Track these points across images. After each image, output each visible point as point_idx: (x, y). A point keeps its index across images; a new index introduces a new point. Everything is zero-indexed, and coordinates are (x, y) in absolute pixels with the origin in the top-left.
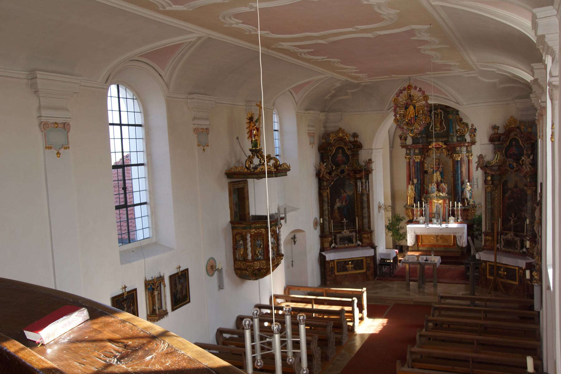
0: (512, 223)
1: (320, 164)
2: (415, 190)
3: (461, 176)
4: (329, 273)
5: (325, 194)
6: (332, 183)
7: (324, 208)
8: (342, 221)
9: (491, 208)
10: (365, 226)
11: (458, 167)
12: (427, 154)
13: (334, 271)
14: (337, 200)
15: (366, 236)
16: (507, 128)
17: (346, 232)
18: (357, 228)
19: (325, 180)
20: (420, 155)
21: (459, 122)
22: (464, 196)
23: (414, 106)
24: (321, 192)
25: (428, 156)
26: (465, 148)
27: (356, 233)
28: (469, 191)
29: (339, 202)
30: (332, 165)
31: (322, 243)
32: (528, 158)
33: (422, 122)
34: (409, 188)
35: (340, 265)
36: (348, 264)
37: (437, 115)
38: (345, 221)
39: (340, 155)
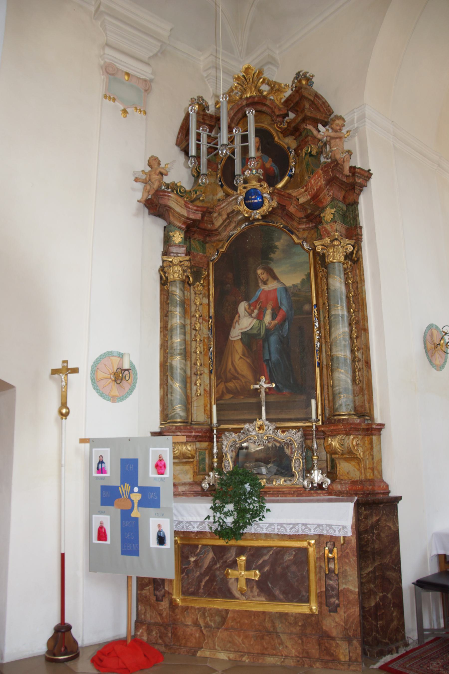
8: (252, 387)
13: (166, 588)
14: (243, 307)
15: (335, 442)
29: (250, 314)
30: (225, 187)
35: (195, 561)
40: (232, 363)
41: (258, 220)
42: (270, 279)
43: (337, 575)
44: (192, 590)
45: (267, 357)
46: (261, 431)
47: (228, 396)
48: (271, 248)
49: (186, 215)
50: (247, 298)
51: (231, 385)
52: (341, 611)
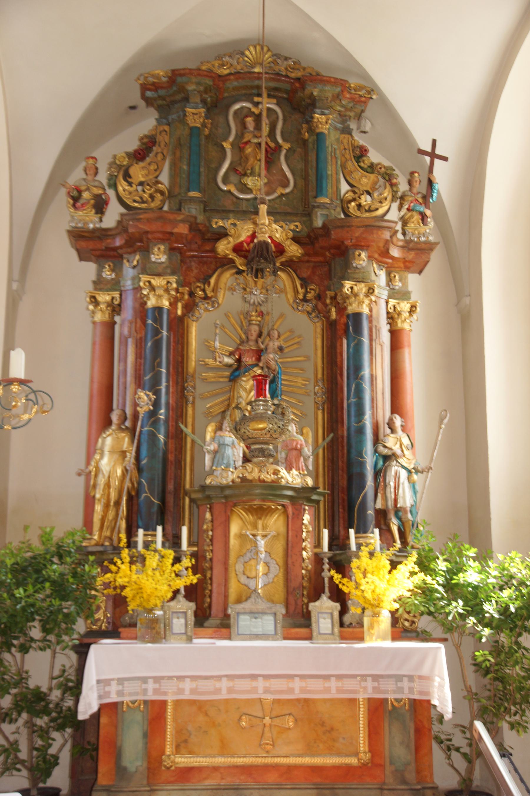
2: (138, 458)
12: (204, 290)
20: (173, 273)
21: (351, 165)
22: (385, 498)
25: (206, 298)
28: (409, 471)
34: (107, 449)
37: (254, 121)
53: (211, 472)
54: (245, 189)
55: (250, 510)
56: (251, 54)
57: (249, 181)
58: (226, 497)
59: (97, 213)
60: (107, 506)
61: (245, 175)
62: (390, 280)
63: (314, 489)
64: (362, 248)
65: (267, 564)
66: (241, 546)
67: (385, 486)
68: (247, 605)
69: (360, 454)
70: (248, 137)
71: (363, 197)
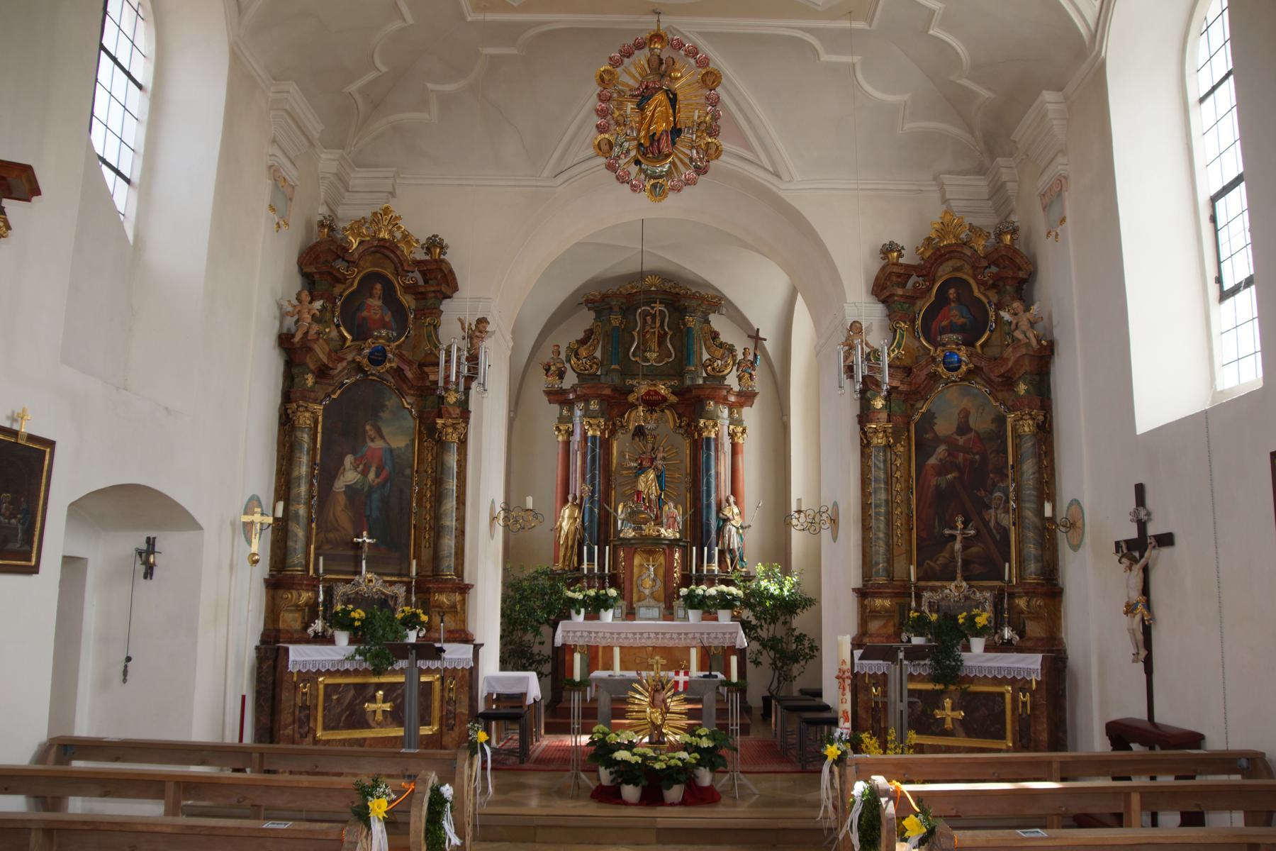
0: (958, 546)
1: (299, 298)
3: (717, 487)
4: (289, 731)
5: (304, 419)
6: (334, 394)
7: (295, 474)
9: (887, 501)
10: (445, 564)
11: (708, 457)
13: (311, 725)
14: (349, 459)
15: (444, 599)
16: (928, 254)
17: (370, 581)
18: (414, 573)
19: (312, 367)
20: (602, 417)
23: (671, 96)
24: (289, 411)
25: (622, 426)
26: (726, 412)
27: (408, 584)
28: (738, 528)
29: (355, 469)
30: (342, 329)
31: (273, 613)
32: (1025, 311)
33: (698, 153)
34: (566, 516)
35: (338, 700)
36: (373, 699)
38: (368, 541)
39: (375, 302)
40: (334, 515)
41: (374, 375)
42: (378, 438)
43: (455, 702)
44: (332, 725)
45: (368, 513)
46: (371, 584)
47: (327, 547)
48: (382, 407)
49: (326, 362)
50: (354, 453)
51: (331, 535)
52: (456, 729)
53: (621, 530)
54: (647, 360)
55: (645, 551)
56: (649, 280)
57: (648, 355)
58: (632, 544)
59: (559, 379)
60: (567, 548)
61: (646, 351)
62: (731, 413)
63: (680, 540)
64: (711, 399)
65: (654, 580)
66: (641, 571)
67: (723, 537)
68: (644, 603)
69: (708, 519)
70: (648, 328)
71: (716, 364)
